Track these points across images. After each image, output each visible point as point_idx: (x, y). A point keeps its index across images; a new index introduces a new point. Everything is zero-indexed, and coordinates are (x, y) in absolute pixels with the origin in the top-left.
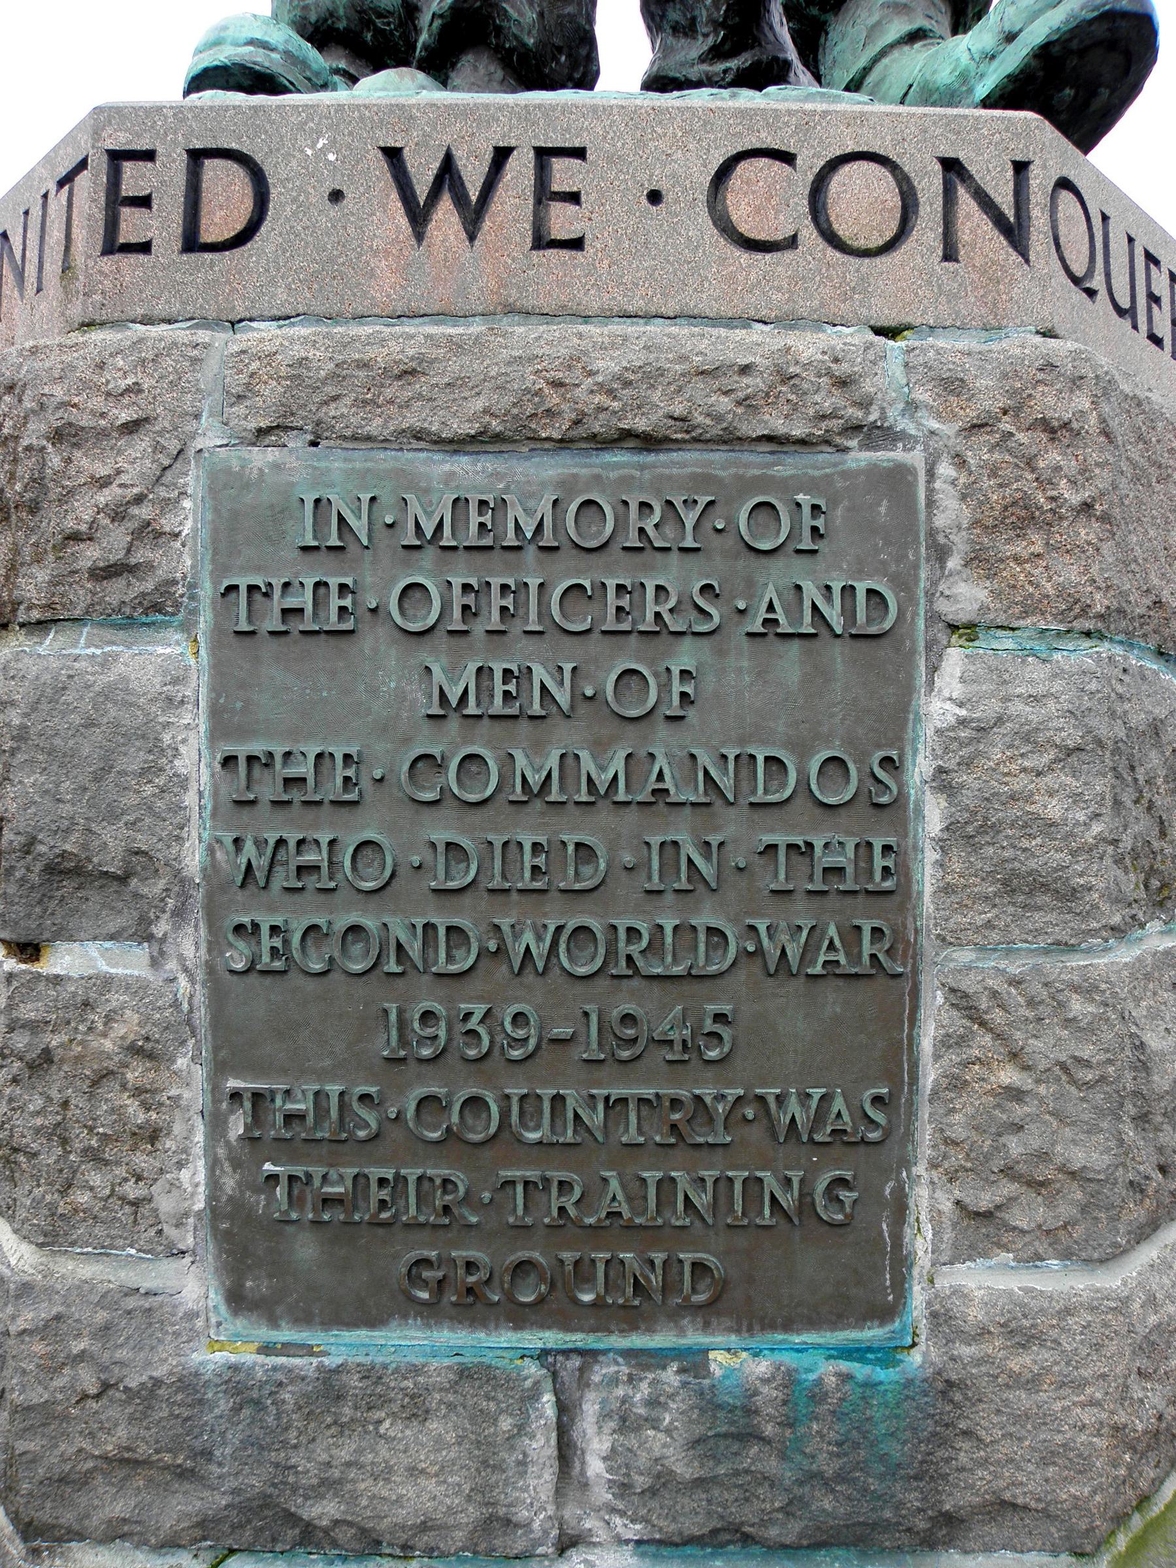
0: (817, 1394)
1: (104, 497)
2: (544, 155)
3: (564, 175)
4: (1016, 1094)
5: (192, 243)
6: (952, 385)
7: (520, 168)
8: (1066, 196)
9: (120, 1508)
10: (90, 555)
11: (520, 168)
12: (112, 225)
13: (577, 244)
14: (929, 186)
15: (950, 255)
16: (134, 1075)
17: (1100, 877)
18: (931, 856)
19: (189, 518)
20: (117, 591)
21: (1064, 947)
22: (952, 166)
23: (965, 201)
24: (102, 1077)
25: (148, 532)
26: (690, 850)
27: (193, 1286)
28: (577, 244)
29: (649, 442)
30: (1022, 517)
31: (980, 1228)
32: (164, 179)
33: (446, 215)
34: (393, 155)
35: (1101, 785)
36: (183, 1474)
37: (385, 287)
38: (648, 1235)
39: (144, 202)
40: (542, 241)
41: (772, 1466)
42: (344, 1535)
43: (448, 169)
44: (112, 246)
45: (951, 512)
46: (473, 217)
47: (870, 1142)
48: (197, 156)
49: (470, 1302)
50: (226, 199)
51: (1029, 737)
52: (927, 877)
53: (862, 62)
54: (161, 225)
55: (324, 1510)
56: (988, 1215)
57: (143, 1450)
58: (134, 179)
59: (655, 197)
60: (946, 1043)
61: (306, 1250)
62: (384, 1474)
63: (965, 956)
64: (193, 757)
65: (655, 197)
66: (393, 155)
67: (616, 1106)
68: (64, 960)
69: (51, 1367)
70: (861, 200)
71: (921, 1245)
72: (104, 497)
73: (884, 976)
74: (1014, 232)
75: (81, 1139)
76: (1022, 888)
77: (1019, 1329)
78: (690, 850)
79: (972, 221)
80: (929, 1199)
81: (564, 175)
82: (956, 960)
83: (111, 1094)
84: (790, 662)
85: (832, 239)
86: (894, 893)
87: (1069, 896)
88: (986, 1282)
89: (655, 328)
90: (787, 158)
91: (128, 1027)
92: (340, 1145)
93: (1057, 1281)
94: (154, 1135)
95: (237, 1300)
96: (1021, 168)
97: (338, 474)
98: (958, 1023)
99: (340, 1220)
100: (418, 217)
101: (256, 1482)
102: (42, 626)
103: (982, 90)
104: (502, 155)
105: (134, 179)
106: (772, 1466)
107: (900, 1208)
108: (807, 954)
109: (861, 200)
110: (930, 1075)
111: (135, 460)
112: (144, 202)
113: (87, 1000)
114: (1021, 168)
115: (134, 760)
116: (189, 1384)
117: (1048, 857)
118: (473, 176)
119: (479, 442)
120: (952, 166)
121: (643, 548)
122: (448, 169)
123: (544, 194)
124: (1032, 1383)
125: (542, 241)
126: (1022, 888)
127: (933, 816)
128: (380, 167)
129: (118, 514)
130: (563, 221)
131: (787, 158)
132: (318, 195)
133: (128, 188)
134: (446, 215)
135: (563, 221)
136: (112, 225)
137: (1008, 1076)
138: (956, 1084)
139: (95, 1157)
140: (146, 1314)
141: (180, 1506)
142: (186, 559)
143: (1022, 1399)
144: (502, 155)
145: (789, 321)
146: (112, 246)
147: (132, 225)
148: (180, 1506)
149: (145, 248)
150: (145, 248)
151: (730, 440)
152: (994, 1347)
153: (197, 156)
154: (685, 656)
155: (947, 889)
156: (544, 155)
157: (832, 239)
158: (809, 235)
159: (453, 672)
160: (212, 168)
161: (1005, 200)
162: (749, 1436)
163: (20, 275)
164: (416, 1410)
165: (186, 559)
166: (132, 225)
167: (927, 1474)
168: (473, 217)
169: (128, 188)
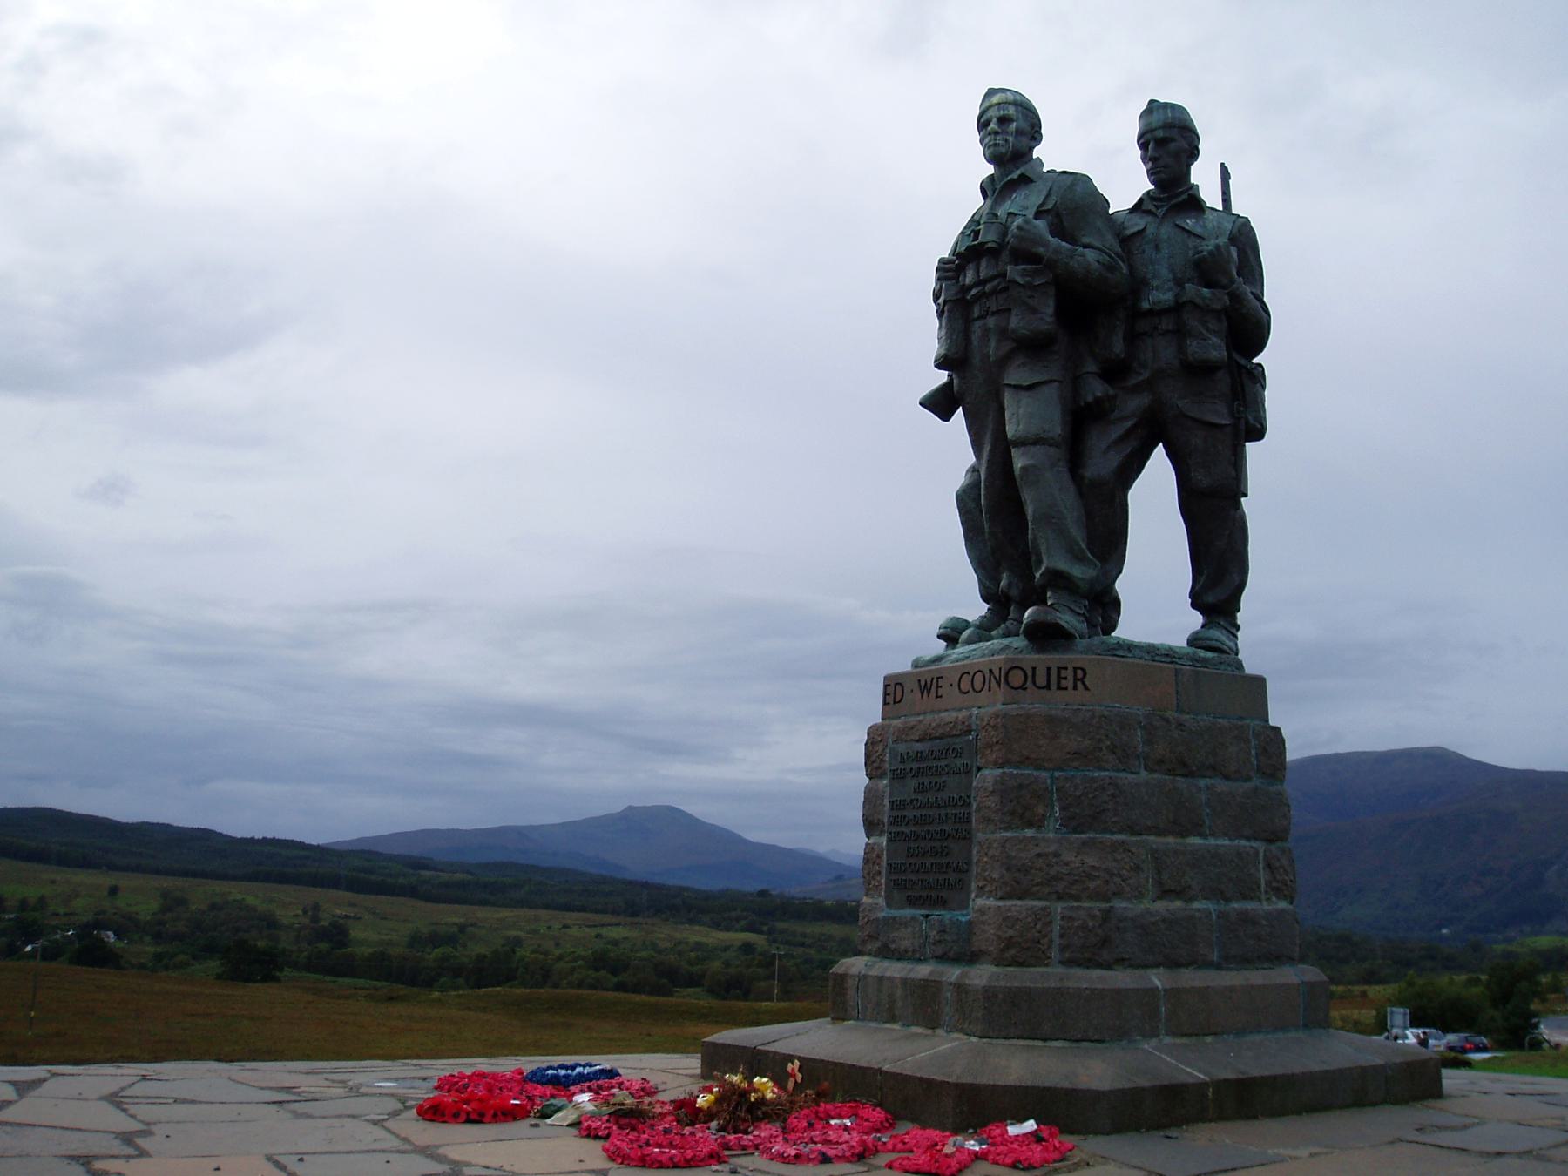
19: (887, 758)
27: (881, 901)
47: (963, 870)
64: (886, 802)
73: (967, 837)
74: (999, 683)
77: (982, 911)
82: (980, 836)
88: (980, 902)
110: (975, 859)
164: (906, 925)
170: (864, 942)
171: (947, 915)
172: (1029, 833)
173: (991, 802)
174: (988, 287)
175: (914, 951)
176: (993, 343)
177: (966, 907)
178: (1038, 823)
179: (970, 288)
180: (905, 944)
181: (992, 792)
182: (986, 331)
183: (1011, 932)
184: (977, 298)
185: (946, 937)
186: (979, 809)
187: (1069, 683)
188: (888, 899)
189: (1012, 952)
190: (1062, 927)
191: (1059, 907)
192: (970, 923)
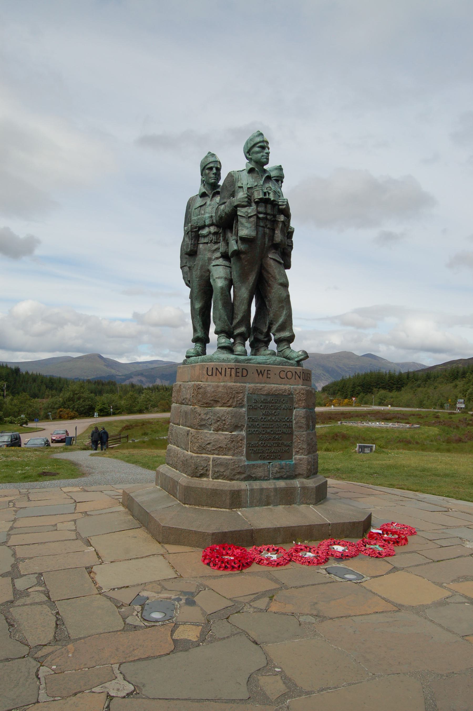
0: (287, 464)
1: (240, 398)
4: (299, 442)
5: (242, 376)
6: (296, 390)
7: (266, 371)
9: (238, 477)
10: (239, 402)
11: (266, 371)
14: (294, 374)
20: (241, 405)
21: (303, 432)
22: (296, 372)
23: (296, 375)
24: (238, 442)
25: (243, 401)
27: (244, 458)
30: (300, 400)
32: (240, 370)
33: (261, 375)
34: (257, 370)
36: (244, 473)
38: (276, 453)
40: (267, 378)
43: (261, 371)
45: (295, 400)
46: (263, 375)
47: (290, 446)
49: (264, 459)
51: (300, 416)
52: (294, 427)
53: (283, 348)
54: (240, 374)
55: (253, 476)
56: (298, 452)
58: (238, 370)
61: (252, 455)
62: (258, 472)
64: (246, 418)
66: (257, 370)
67: (274, 443)
69: (234, 465)
70: (289, 375)
71: (294, 454)
72: (240, 398)
73: (291, 434)
74: (300, 377)
75: (236, 447)
76: (300, 427)
77: (300, 460)
80: (294, 450)
82: (295, 433)
84: (285, 411)
86: (292, 428)
88: (298, 457)
89: (276, 385)
91: (240, 438)
92: (255, 447)
93: (303, 456)
94: (241, 446)
95: (247, 459)
97: (255, 397)
99: (255, 453)
100: (259, 375)
101: (249, 473)
102: (234, 407)
103: (296, 360)
105: (238, 370)
107: (292, 451)
109: (289, 375)
115: (242, 418)
116: (244, 466)
119: (266, 395)
120: (296, 372)
121: (276, 403)
122: (261, 371)
123: (267, 374)
124: (301, 464)
125: (267, 378)
126: (300, 427)
127: (294, 422)
128: (256, 371)
129: (241, 399)
130: (269, 376)
134: (261, 375)
135: (269, 376)
140: (240, 461)
141: (243, 476)
142: (245, 402)
145: (284, 384)
148: (243, 476)
154: (278, 411)
156: (268, 370)
162: (283, 468)
163: (221, 373)
165: (245, 402)
168: (263, 375)
170: (235, 475)
171: (283, 462)
173: (303, 421)
174: (268, 217)
175: (264, 477)
176: (267, 240)
177: (291, 458)
180: (260, 474)
181: (303, 418)
185: (283, 470)
186: (296, 423)
188: (248, 458)
192: (296, 464)
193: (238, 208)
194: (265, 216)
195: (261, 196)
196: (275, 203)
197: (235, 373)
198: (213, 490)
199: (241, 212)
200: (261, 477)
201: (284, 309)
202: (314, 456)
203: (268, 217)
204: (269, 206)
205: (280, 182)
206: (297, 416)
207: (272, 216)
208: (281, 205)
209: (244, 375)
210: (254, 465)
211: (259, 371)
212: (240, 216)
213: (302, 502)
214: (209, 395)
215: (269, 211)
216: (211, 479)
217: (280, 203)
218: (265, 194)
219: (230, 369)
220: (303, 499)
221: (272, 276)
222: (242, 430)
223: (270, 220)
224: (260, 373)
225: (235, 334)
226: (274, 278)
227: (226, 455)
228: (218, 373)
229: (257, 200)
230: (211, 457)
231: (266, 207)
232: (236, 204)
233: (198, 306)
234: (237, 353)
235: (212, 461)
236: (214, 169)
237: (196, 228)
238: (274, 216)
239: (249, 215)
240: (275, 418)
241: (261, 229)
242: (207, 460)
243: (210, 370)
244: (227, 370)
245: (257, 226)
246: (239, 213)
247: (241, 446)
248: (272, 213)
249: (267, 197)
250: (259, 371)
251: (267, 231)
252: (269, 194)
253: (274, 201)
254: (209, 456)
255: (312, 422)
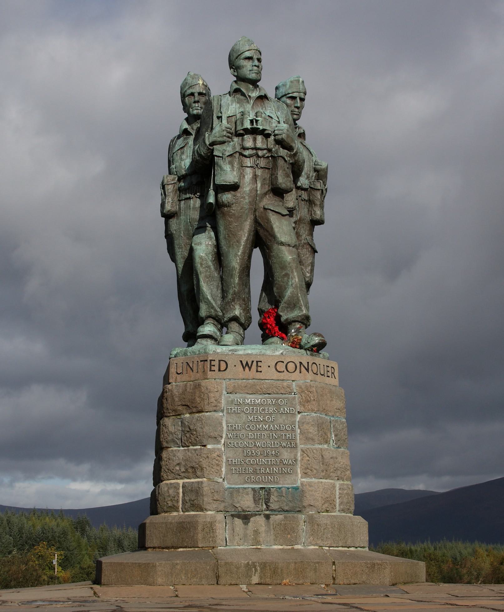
2: (257, 362)
3: (259, 364)
4: (309, 460)
5: (219, 370)
7: (255, 363)
8: (314, 365)
10: (213, 404)
11: (255, 363)
12: (211, 368)
13: (261, 372)
14: (298, 365)
15: (300, 373)
16: (218, 458)
17: (316, 438)
18: (298, 435)
22: (301, 363)
25: (219, 402)
26: (274, 435)
28: (261, 372)
29: (269, 394)
30: (308, 401)
31: (305, 474)
32: (216, 363)
34: (241, 361)
35: (316, 428)
37: (241, 376)
39: (214, 366)
40: (257, 371)
41: (285, 499)
42: (240, 508)
44: (210, 370)
46: (250, 369)
48: (220, 361)
50: (223, 366)
51: (308, 423)
54: (216, 368)
57: (219, 499)
58: (213, 363)
59: (269, 366)
60: (301, 455)
63: (303, 446)
65: (269, 366)
66: (241, 361)
68: (209, 447)
70: (291, 367)
74: (307, 370)
77: (310, 484)
78: (274, 435)
79: (303, 369)
81: (259, 364)
82: (300, 446)
83: (214, 460)
85: (288, 371)
86: (295, 439)
87: (313, 440)
90: (283, 362)
93: (314, 480)
96: (308, 363)
98: (302, 453)
100: (244, 368)
104: (253, 362)
105: (213, 363)
106: (285, 499)
108: (287, 445)
109: (291, 367)
110: (299, 459)
111: (217, 395)
112: (214, 366)
113: (213, 450)
114: (308, 363)
117: (310, 436)
118: (250, 364)
120: (301, 363)
124: (312, 491)
125: (257, 371)
126: (307, 439)
128: (240, 363)
130: (259, 369)
131: (283, 362)
132: (233, 366)
133: (212, 364)
134: (247, 368)
136: (211, 368)
137: (308, 458)
138: (302, 460)
139: (212, 468)
143: (311, 493)
144: (253, 362)
146: (210, 370)
147: (213, 368)
149: (214, 371)
150: (214, 371)
151: (277, 394)
152: (308, 487)
153: (220, 361)
155: (300, 439)
156: (257, 362)
157: (288, 371)
158: (285, 370)
159: (251, 417)
160: (221, 362)
161: (306, 366)
166: (213, 368)
167: (301, 501)
168: (250, 369)
169: (212, 364)
172: (326, 446)
174: (260, 153)
176: (259, 185)
178: (327, 442)
179: (248, 149)
182: (255, 177)
183: (326, 496)
184: (250, 156)
187: (330, 374)
189: (326, 505)
190: (340, 494)
191: (338, 484)
193: (215, 147)
194: (255, 151)
195: (248, 125)
196: (266, 132)
197: (209, 366)
198: (180, 523)
199: (218, 150)
200: (248, 507)
201: (289, 278)
202: (341, 485)
203: (260, 153)
204: (259, 138)
205: (298, 99)
206: (303, 423)
207: (265, 151)
208: (277, 135)
209: (223, 368)
210: (238, 490)
211: (244, 364)
212: (217, 156)
213: (310, 543)
214: (177, 399)
215: (259, 144)
216: (182, 513)
217: (276, 132)
218: (252, 121)
219: (202, 362)
220: (312, 538)
221: (270, 234)
222: (219, 442)
223: (263, 157)
224: (246, 366)
225: (225, 319)
226: (273, 236)
227: (198, 477)
228: (189, 369)
229: (239, 132)
230: (181, 482)
231: (255, 140)
232: (211, 142)
233: (184, 288)
234: (222, 343)
235: (183, 487)
236: (196, 95)
237: (173, 180)
238: (269, 150)
239: (227, 154)
240: (269, 426)
241: (249, 171)
242: (176, 487)
243: (180, 365)
244: (200, 363)
245: (242, 166)
246: (215, 153)
247: (218, 465)
248: (265, 147)
249: (255, 126)
250: (244, 364)
251: (259, 172)
252: (257, 121)
253: (264, 130)
254: (178, 481)
255: (336, 436)
